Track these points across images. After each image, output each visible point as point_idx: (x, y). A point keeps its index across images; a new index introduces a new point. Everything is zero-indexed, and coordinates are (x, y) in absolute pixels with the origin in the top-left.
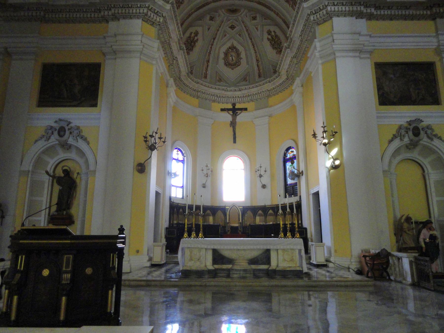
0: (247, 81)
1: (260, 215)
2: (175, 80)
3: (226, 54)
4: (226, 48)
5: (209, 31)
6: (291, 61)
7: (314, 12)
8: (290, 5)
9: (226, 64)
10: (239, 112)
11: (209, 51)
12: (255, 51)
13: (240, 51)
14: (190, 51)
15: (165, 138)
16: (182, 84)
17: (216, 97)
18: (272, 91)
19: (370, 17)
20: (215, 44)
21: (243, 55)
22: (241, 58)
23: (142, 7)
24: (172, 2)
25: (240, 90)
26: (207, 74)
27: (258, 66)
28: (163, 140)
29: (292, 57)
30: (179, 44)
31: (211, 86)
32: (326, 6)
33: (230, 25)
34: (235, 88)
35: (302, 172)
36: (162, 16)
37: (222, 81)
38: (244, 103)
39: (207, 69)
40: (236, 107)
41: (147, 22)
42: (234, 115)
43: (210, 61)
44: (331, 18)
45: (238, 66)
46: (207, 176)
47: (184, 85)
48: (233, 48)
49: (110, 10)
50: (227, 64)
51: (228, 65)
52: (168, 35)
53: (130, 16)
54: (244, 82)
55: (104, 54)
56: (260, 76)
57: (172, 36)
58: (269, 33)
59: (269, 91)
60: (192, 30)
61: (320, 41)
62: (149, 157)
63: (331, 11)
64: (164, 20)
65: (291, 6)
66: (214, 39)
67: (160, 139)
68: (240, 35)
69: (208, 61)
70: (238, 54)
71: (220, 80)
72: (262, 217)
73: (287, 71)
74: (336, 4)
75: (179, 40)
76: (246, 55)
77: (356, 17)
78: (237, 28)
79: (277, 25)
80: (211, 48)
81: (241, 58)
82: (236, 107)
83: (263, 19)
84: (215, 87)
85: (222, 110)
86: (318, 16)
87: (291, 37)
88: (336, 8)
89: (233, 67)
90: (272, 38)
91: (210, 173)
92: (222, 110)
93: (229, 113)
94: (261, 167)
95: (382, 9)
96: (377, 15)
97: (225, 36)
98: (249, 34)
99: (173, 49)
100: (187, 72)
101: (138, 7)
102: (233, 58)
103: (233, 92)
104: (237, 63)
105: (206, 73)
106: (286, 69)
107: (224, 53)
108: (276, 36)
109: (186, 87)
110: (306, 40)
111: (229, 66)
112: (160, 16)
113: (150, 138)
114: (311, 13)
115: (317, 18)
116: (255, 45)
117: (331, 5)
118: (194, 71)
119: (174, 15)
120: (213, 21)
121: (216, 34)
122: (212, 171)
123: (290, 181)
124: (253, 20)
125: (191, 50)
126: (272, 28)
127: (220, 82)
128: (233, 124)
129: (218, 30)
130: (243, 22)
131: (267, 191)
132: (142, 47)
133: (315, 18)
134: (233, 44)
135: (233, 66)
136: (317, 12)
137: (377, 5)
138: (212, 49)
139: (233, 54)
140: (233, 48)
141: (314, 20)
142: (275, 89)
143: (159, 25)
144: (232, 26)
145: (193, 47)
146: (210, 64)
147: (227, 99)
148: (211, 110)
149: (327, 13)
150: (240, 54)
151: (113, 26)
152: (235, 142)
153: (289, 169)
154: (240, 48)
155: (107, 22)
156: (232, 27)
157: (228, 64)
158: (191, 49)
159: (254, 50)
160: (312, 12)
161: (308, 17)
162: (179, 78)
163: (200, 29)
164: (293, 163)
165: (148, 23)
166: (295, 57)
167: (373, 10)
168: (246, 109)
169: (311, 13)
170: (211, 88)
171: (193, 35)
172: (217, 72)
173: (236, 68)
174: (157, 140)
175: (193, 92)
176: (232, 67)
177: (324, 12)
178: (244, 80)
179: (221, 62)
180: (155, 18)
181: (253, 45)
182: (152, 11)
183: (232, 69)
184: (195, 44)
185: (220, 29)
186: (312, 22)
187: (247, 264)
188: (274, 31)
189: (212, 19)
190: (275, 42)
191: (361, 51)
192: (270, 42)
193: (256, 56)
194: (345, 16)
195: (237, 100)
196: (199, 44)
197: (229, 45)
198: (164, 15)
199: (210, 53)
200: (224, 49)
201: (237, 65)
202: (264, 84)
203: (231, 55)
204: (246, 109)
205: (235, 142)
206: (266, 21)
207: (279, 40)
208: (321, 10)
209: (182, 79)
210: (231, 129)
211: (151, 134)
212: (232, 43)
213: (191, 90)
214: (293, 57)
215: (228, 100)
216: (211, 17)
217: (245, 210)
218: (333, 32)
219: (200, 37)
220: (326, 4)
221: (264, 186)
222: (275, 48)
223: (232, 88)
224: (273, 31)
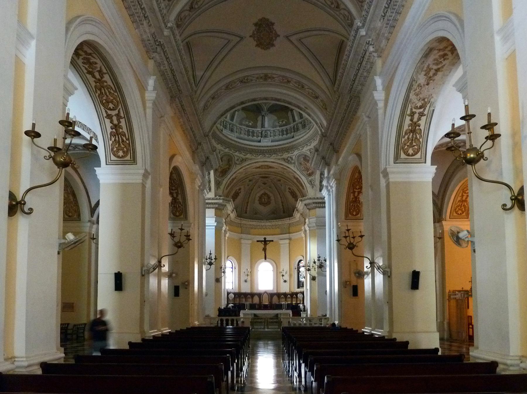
3: (260, 198)
9: (260, 203)
21: (272, 198)
27: (283, 205)
48: (265, 194)
69: (248, 203)
76: (274, 198)
125: (236, 198)
140: (265, 194)
146: (249, 204)
156: (265, 184)
157: (261, 203)
179: (257, 202)
183: (265, 206)
200: (259, 195)
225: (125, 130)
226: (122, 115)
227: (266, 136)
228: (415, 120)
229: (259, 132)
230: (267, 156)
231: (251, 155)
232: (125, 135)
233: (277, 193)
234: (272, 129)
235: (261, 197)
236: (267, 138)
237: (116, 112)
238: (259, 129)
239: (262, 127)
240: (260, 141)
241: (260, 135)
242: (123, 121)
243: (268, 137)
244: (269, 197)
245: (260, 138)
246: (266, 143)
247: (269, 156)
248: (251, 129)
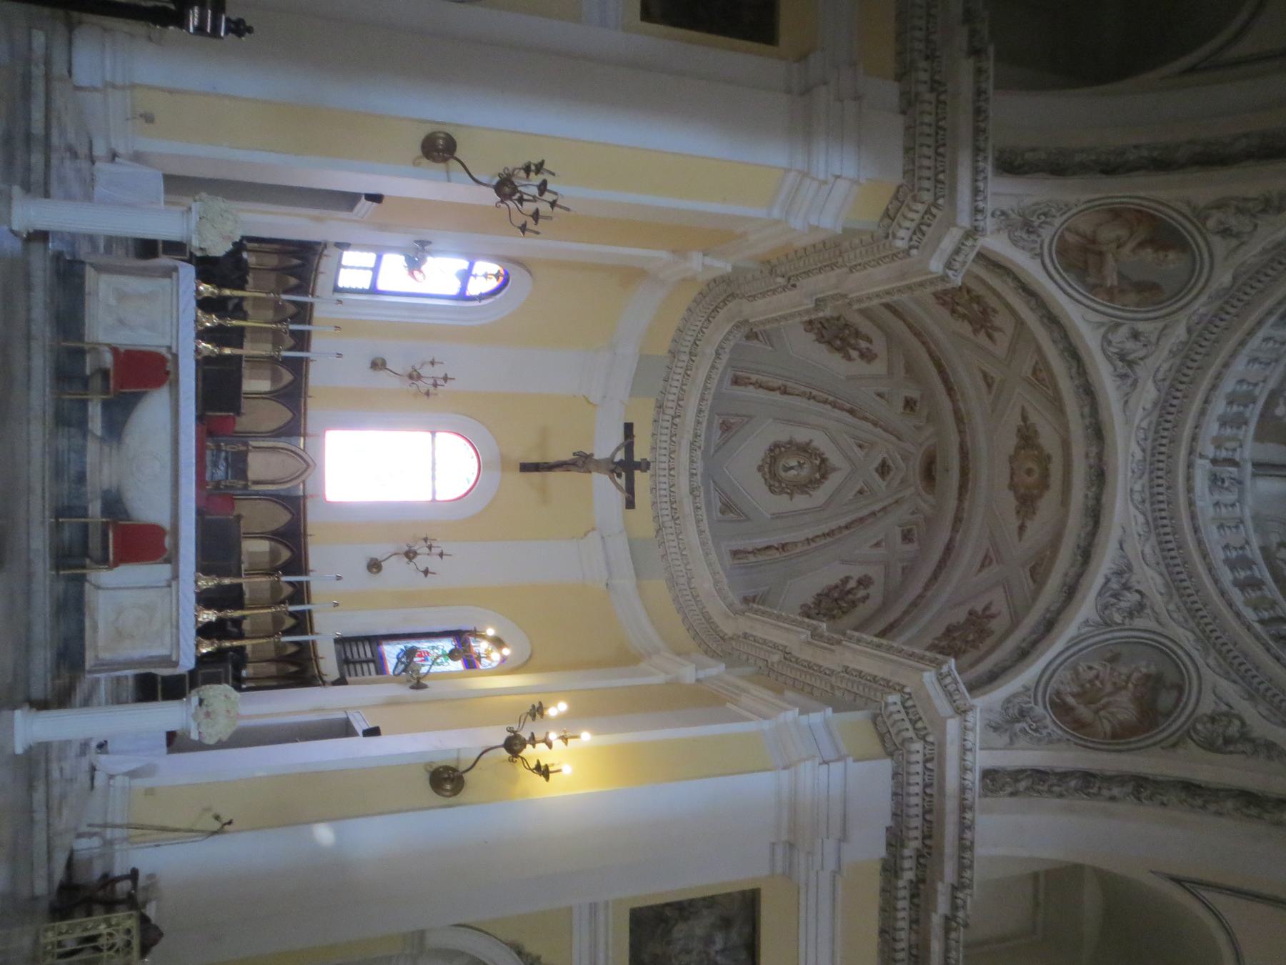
0: (722, 512)
1: (274, 554)
2: (725, 280)
3: (805, 449)
4: (822, 450)
5: (875, 396)
6: (775, 646)
7: (910, 703)
8: (937, 639)
10: (622, 481)
11: (814, 393)
12: (813, 540)
13: (812, 493)
14: (815, 334)
15: (537, 233)
16: (715, 304)
17: (671, 412)
18: (688, 592)
19: (891, 869)
20: (837, 413)
21: (801, 502)
22: (791, 495)
23: (936, 187)
24: (948, 276)
25: (692, 491)
26: (746, 385)
27: (768, 548)
28: (531, 222)
29: (786, 647)
30: (834, 297)
31: (709, 397)
32: (923, 738)
33: (892, 465)
34: (699, 477)
35: (425, 687)
36: (911, 247)
37: (722, 434)
38: (654, 503)
39: (761, 386)
40: (637, 474)
41: (896, 197)
42: (613, 467)
43: (786, 396)
44: (891, 755)
45: (770, 486)
46: (411, 377)
47: (712, 307)
48: (823, 469)
49: (932, 90)
50: (777, 451)
51: (772, 454)
52: (859, 261)
53: (913, 148)
54: (719, 504)
55: (803, 57)
56: (735, 553)
57: (856, 275)
58: (864, 582)
59: (689, 583)
60: (879, 345)
61: (826, 724)
62: (475, 176)
63: (910, 752)
64: (899, 253)
65: (936, 642)
66: (851, 412)
67: (532, 216)
68: (861, 492)
69: (785, 392)
70: (805, 486)
71: (726, 427)
72: (267, 559)
73: (746, 636)
74: (929, 765)
75: (845, 296)
76: (805, 512)
77: (891, 827)
78: (883, 484)
79: (885, 606)
80: (825, 402)
81: (791, 495)
82: (637, 474)
83: (905, 564)
84: (703, 412)
85: (629, 428)
86: (897, 717)
87: (844, 643)
88: (919, 768)
89: (766, 470)
90: (849, 592)
91: (424, 385)
92: (629, 428)
93: (618, 449)
94: (441, 555)
95: (911, 902)
96: (896, 888)
97: (860, 446)
98: (861, 520)
99: (821, 277)
100: (751, 321)
101: (936, 175)
102: (793, 472)
103: (688, 468)
104: (777, 484)
105: (751, 384)
106: (754, 633)
107: (811, 441)
108: (854, 604)
109: (706, 316)
110: (832, 687)
111: (771, 457)
112: (911, 239)
113: (538, 183)
114: (907, 696)
115: (891, 714)
116: (829, 539)
117: (927, 751)
118: (755, 343)
119: (914, 284)
120: (905, 408)
121: (866, 419)
122: (428, 394)
123: (391, 652)
124: (903, 531)
125: (821, 339)
126: (876, 592)
127: (721, 428)
128: (582, 462)
129: (875, 424)
130: (896, 502)
131: (358, 577)
132: (822, 177)
133: (892, 708)
134: (834, 469)
135: (770, 472)
136: (907, 713)
137: (921, 886)
138: (822, 405)
139: (805, 472)
140: (823, 469)
141: (887, 705)
142: (693, 603)
143: (887, 237)
144: (889, 466)
145: (829, 343)
146: (776, 396)
147: (665, 449)
148: (630, 396)
149: (904, 741)
150: (807, 493)
151: (889, 91)
152: (526, 468)
153: (433, 648)
154: (820, 495)
155: (899, 77)
156: (884, 469)
157: (776, 452)
158: (823, 336)
159: (818, 536)
160: (910, 698)
161: (897, 688)
162: (733, 296)
163: (879, 367)
164: (452, 655)
165: (891, 203)
166: (787, 655)
167: (909, 875)
168: (630, 504)
169: (907, 696)
170: (702, 399)
171: (863, 344)
172: (750, 417)
173: (763, 480)
174: (529, 207)
175: (689, 338)
176: (767, 465)
177: (911, 734)
178: (723, 504)
180: (907, 224)
181: (830, 534)
182: (926, 217)
183: (760, 468)
184: (838, 350)
185: (879, 430)
186: (882, 699)
187: (106, 486)
188: (866, 597)
189: (909, 404)
190: (836, 600)
191: (791, 846)
192: (836, 587)
193: (795, 544)
194: (895, 794)
195: (663, 479)
196: (834, 364)
197: (834, 458)
198: (914, 252)
199: (811, 397)
200: (820, 442)
201: (772, 483)
202: (710, 565)
203: (804, 463)
204: (630, 504)
205: (526, 468)
206: (900, 570)
207: (843, 612)
208: (913, 722)
209: (730, 305)
210: (567, 456)
211: (549, 187)
212: (839, 469)
213: (695, 334)
214: (787, 650)
215: (663, 452)
216: (915, 403)
217: (294, 504)
218: (850, 760)
219: (859, 367)
220: (930, 739)
221: (375, 566)
222: (820, 601)
223: (699, 466)
224: (868, 594)
229: (1234, 450)
230: (1137, 487)
231: (1149, 406)
233: (833, 525)
234: (1248, 513)
235: (805, 451)
236: (1207, 491)
238: (1250, 451)
239: (1257, 465)
241: (1223, 454)
243: (1211, 493)
244: (805, 487)
245: (1211, 456)
247: (1137, 497)
248: (1254, 413)
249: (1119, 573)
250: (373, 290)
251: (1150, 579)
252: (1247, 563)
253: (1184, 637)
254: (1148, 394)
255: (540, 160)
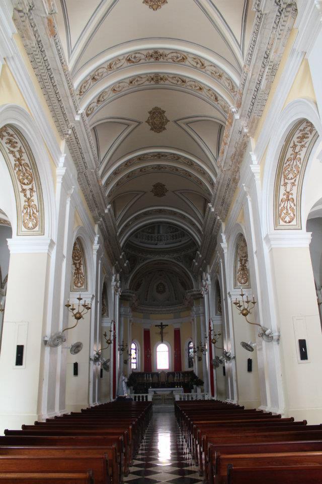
9: (157, 291)
21: (166, 287)
48: (161, 284)
56: (176, 299)
58: (179, 280)
85: (156, 326)
92: (156, 326)
140: (161, 284)
156: (161, 275)
157: (159, 292)
168: (167, 325)
225: (82, 271)
226: (82, 263)
227: (161, 240)
228: (243, 263)
232: (82, 274)
237: (79, 261)
238: (156, 235)
240: (156, 244)
242: (82, 266)
246: (161, 245)
249: (175, 259)
250: (136, 363)
251: (175, 255)
252: (173, 236)
253: (183, 253)
254: (149, 256)
255: (78, 300)
